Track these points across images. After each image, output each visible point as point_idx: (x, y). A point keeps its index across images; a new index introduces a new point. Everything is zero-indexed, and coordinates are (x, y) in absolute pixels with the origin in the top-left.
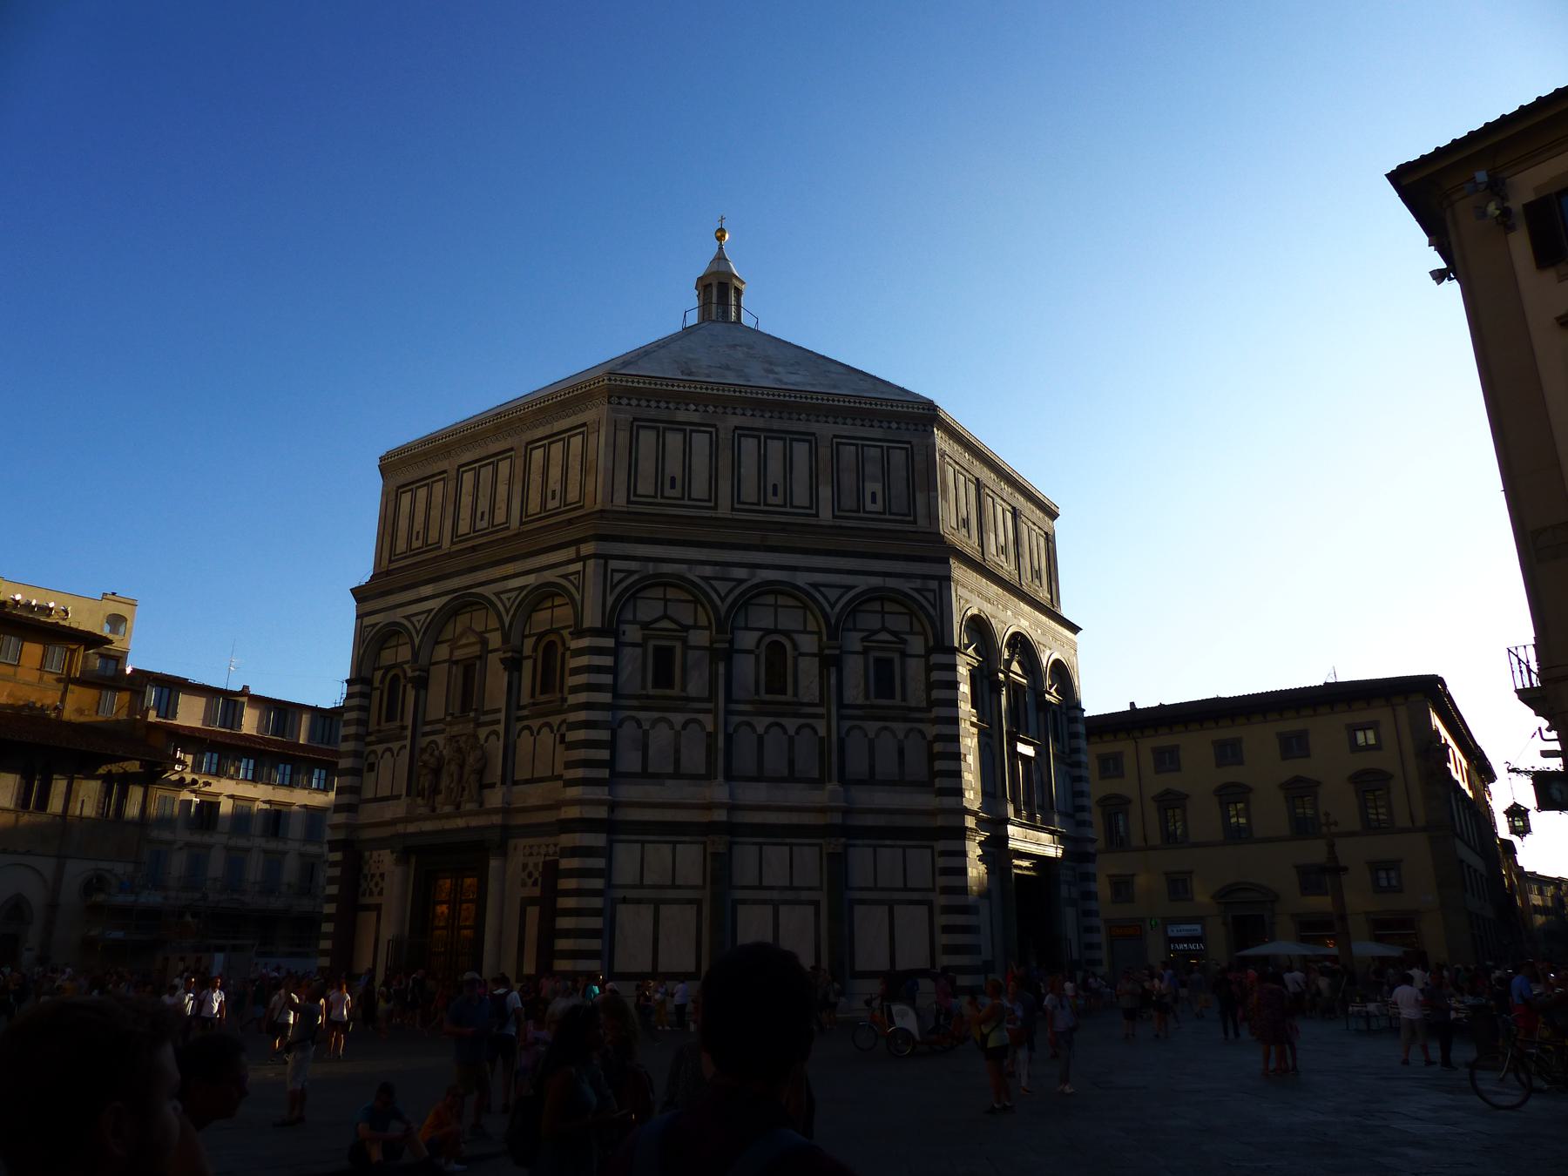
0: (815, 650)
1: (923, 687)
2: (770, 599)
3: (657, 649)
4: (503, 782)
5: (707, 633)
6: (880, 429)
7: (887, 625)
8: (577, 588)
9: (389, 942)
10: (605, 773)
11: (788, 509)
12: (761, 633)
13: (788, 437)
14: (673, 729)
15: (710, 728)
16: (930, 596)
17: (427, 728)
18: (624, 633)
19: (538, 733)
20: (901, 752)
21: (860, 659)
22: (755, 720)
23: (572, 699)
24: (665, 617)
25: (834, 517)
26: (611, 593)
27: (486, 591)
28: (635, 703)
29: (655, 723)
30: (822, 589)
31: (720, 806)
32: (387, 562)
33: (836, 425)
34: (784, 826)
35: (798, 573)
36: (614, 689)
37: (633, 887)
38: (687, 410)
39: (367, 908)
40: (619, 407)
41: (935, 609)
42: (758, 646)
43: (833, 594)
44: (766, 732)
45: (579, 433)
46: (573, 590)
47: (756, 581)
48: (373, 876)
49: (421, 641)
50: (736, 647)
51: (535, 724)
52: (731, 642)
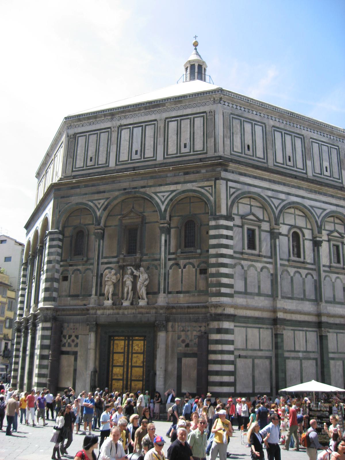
0: (311, 238)
2: (292, 211)
3: (249, 229)
4: (164, 292)
5: (268, 224)
7: (336, 229)
8: (211, 195)
9: (92, 372)
11: (295, 169)
13: (293, 134)
15: (272, 272)
17: (105, 260)
19: (184, 267)
22: (289, 269)
23: (212, 251)
26: (230, 199)
27: (148, 191)
28: (241, 256)
32: (71, 171)
33: (310, 133)
35: (305, 200)
37: (243, 350)
38: (252, 113)
39: (67, 353)
40: (224, 106)
43: (319, 211)
46: (209, 195)
47: (289, 201)
48: (70, 337)
49: (102, 213)
51: (182, 262)
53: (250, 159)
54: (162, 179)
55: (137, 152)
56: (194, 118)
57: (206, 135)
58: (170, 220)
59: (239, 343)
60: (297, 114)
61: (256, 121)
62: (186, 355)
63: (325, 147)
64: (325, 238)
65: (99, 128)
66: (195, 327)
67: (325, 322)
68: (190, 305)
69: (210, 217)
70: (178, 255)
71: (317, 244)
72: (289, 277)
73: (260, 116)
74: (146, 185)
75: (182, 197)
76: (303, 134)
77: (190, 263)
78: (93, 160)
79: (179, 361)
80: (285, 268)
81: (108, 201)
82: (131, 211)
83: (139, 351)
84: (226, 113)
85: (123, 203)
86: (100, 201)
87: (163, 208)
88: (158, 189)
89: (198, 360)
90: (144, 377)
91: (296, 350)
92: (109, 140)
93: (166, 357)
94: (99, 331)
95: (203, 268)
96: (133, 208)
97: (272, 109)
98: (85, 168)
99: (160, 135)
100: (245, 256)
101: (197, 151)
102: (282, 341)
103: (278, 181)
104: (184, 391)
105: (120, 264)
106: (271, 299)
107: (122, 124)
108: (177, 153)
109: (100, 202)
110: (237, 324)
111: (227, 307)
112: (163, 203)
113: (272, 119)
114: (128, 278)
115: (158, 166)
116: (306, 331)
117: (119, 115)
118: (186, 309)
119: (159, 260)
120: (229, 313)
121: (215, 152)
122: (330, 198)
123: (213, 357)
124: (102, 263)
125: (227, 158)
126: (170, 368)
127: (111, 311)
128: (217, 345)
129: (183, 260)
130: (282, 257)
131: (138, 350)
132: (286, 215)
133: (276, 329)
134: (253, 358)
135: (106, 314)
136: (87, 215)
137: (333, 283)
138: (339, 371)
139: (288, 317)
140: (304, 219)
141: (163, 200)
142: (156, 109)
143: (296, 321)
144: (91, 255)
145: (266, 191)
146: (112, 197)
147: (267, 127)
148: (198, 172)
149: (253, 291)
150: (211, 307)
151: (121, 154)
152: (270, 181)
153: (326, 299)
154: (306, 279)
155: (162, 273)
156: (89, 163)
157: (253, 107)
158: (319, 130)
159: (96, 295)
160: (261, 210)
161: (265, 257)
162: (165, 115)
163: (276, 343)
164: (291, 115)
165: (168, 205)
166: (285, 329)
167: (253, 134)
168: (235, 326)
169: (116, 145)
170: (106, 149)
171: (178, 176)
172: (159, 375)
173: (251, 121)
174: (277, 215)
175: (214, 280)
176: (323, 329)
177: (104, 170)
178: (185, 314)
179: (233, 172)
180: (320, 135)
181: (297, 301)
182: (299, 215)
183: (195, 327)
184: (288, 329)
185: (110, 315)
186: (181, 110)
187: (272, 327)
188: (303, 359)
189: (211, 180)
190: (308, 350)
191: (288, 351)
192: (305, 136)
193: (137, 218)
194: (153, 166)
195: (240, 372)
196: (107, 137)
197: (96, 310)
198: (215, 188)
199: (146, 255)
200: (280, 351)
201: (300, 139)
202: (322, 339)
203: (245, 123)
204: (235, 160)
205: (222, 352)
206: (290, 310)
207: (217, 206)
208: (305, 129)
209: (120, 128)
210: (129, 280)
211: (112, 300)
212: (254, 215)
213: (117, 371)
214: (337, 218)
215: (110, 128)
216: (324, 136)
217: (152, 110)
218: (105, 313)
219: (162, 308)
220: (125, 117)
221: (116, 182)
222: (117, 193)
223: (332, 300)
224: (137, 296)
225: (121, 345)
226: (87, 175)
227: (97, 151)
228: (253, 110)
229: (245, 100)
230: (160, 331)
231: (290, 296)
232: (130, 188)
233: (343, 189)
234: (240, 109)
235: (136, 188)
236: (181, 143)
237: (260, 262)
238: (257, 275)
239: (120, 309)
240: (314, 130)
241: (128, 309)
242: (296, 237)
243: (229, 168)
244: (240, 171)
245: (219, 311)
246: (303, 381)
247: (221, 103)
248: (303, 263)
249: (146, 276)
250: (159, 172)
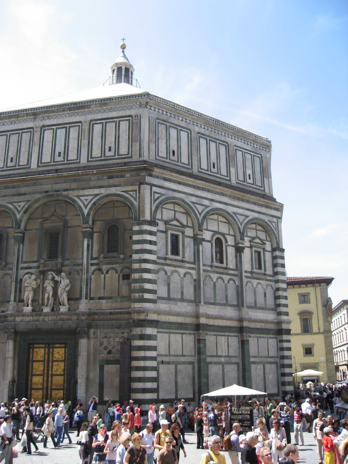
0: (234, 244)
1: (271, 266)
2: (215, 217)
3: (172, 235)
4: (86, 298)
5: (192, 230)
6: (251, 146)
8: (135, 199)
9: (9, 382)
11: (219, 176)
12: (212, 233)
13: (218, 142)
15: (195, 277)
16: (274, 224)
17: (25, 265)
19: (107, 273)
20: (265, 294)
23: (135, 257)
27: (71, 194)
28: (164, 262)
30: (236, 215)
33: (235, 140)
35: (228, 206)
37: (166, 356)
38: (178, 119)
40: (150, 110)
41: (276, 231)
43: (241, 218)
44: (217, 281)
45: (127, 120)
49: (22, 216)
51: (104, 268)
53: (174, 164)
54: (86, 182)
55: (60, 153)
56: (119, 121)
57: (131, 140)
58: (93, 224)
59: (162, 349)
60: (222, 122)
61: (182, 127)
62: (108, 362)
63: (248, 155)
64: (247, 244)
65: (21, 127)
66: (118, 333)
67: (246, 327)
68: (112, 311)
69: (133, 222)
70: (101, 260)
71: (239, 250)
72: (212, 283)
73: (186, 122)
74: (69, 188)
75: (106, 201)
76: (227, 141)
77: (113, 269)
78: (14, 160)
79: (102, 368)
80: (208, 274)
81: (29, 203)
82: (53, 215)
83: (60, 359)
84: (151, 117)
85: (44, 206)
86: (20, 204)
87: (86, 212)
88: (81, 192)
89: (120, 366)
90: (65, 385)
91: (218, 355)
92: (31, 140)
93: (88, 364)
94: (18, 339)
95: (126, 273)
96: (55, 211)
97: (198, 116)
98: (5, 169)
99: (84, 137)
100: (169, 262)
101: (122, 155)
102: (205, 347)
103: (202, 188)
104: (106, 399)
105: (40, 269)
106: (194, 304)
107: (45, 124)
108: (101, 157)
109: (20, 204)
110: (160, 330)
111: (150, 313)
112: (86, 207)
113: (197, 126)
114: (49, 284)
115: (82, 169)
116: (228, 336)
117: (42, 116)
118: (109, 316)
119: (82, 265)
120: (152, 319)
121: (140, 156)
122: (253, 205)
123: (135, 364)
124: (22, 268)
125: (152, 163)
126: (92, 376)
127: (30, 318)
128: (140, 352)
129: (106, 266)
130: (205, 263)
131: (58, 357)
132: (209, 221)
133: (199, 335)
134: (176, 364)
135: (25, 321)
136: (6, 217)
137: (255, 288)
138: (259, 375)
139: (211, 322)
140: (227, 225)
141: (86, 203)
142: (81, 111)
144: (10, 259)
145: (191, 197)
146: (33, 200)
147: (193, 133)
148: (122, 176)
149: (176, 297)
150: (134, 313)
151: (43, 156)
152: (194, 187)
153: (247, 305)
154: (228, 285)
155: (84, 278)
156: (10, 164)
157: (178, 113)
158: (243, 138)
159: (15, 301)
160: (185, 216)
161: (188, 262)
162: (90, 117)
163: (199, 349)
164: (217, 123)
165: (91, 209)
166: (207, 335)
167: (178, 139)
168: (158, 332)
169: (38, 147)
170: (27, 150)
171: (101, 179)
172: (81, 383)
173: (177, 127)
175: (137, 285)
176: (244, 334)
177: (26, 171)
178: (107, 320)
179: (157, 178)
180: (244, 143)
181: (220, 307)
182: (222, 222)
183: (118, 333)
184: (211, 335)
185: (29, 322)
186: (107, 113)
187: (195, 332)
188: (225, 364)
189: (135, 185)
190: (230, 355)
191: (210, 356)
192: (229, 143)
193: (58, 222)
194: (77, 169)
195: (163, 379)
196: (29, 137)
197: (15, 316)
198: (139, 192)
199: (68, 260)
200: (202, 357)
201: (225, 147)
202: (243, 344)
203: (171, 129)
204: (159, 165)
205: (145, 358)
206: (212, 315)
207: (141, 210)
208: (230, 136)
209: (43, 128)
210: (50, 285)
211: (32, 307)
212: (178, 221)
213: (37, 380)
214: (259, 225)
215: (32, 128)
216: (247, 144)
217: (76, 111)
218: (24, 320)
219: (83, 314)
220: (48, 117)
221: (37, 184)
222: (38, 196)
223: (253, 305)
224: (58, 302)
225: (41, 353)
226: (7, 177)
227: (19, 151)
228: (179, 115)
229: (171, 106)
230: (82, 338)
231: (213, 301)
232: (52, 191)
233: (265, 197)
234: (166, 115)
235: (58, 191)
236: (106, 146)
237: (184, 267)
238: (180, 280)
239: (40, 316)
240: (238, 138)
241: (49, 315)
242: (219, 242)
243: (154, 173)
244: (165, 176)
245: (142, 317)
246: (225, 385)
247: (147, 108)
248: (226, 268)
249: (67, 281)
250: (83, 175)
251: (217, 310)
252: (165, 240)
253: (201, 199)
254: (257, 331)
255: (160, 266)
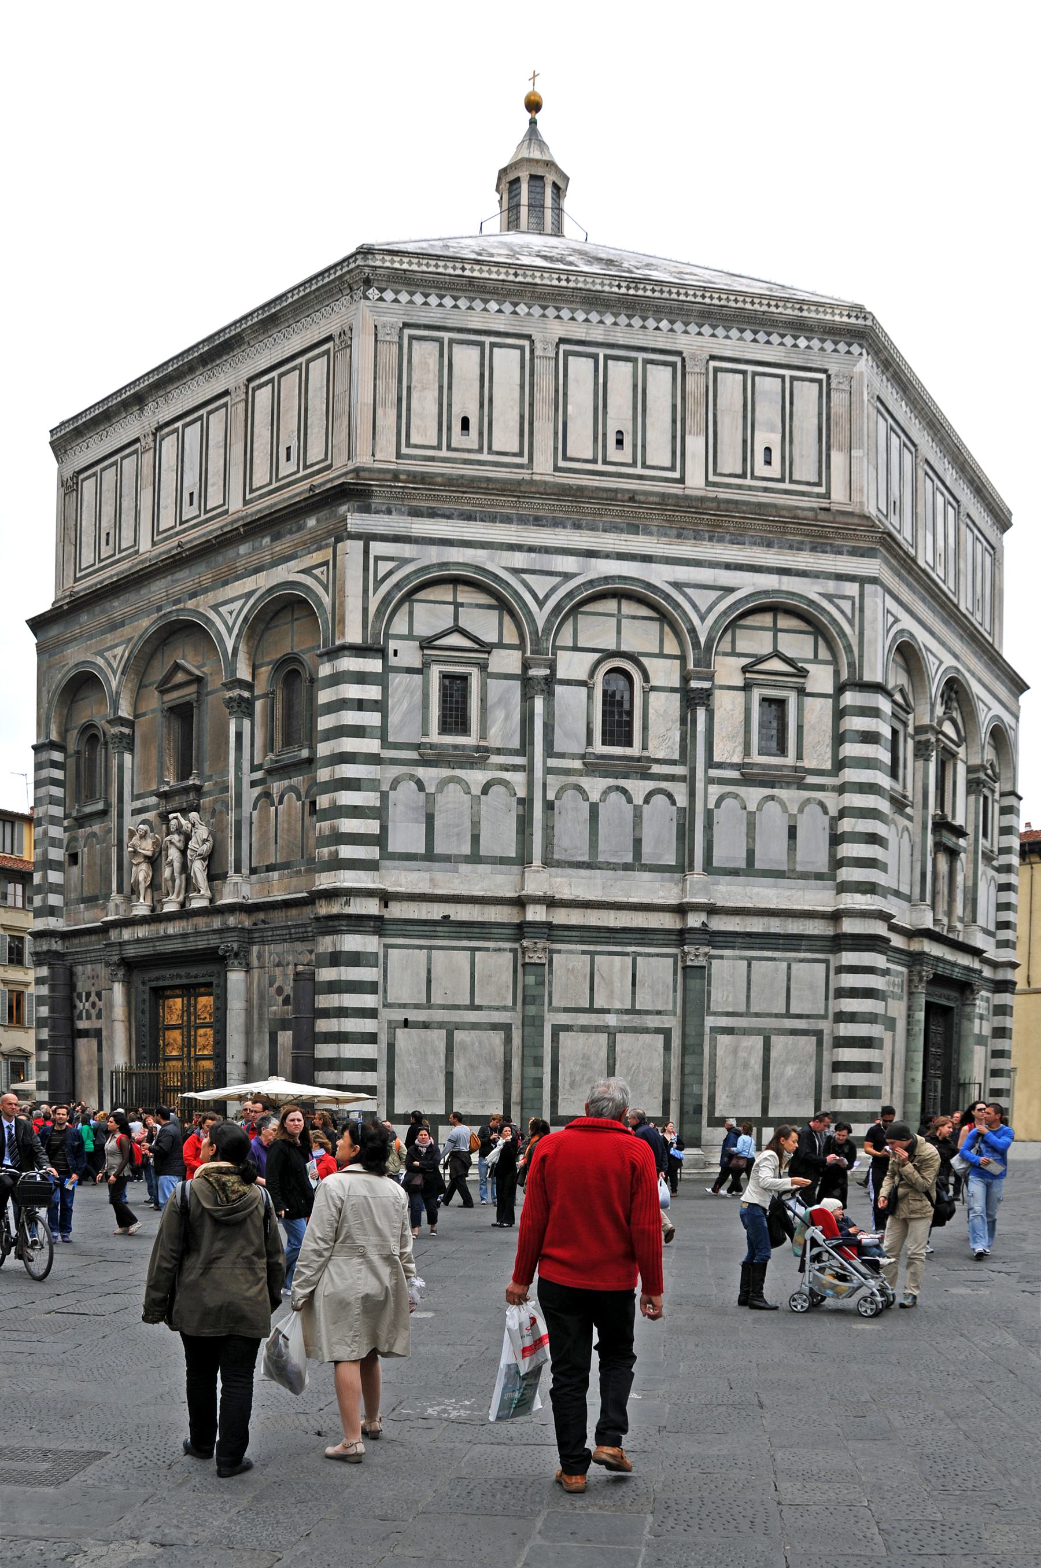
2: (611, 605)
5: (517, 655)
10: (371, 852)
11: (639, 471)
12: (597, 656)
14: (469, 793)
15: (521, 793)
18: (396, 653)
21: (742, 693)
22: (585, 782)
24: (458, 630)
25: (708, 483)
28: (413, 755)
29: (444, 783)
31: (536, 900)
34: (625, 930)
36: (382, 733)
41: (851, 622)
42: (592, 673)
44: (603, 799)
50: (560, 675)
52: (552, 666)
72: (587, 804)
80: (572, 779)
106: (516, 869)
139: (562, 917)
143: (598, 929)
149: (453, 851)
161: (499, 751)
174: (540, 624)
182: (634, 617)
184: (571, 952)
231: (585, 858)
238: (468, 804)
248: (639, 759)
251: (599, 882)
252: (419, 694)
253: (546, 557)
254: (748, 940)
255: (395, 771)
